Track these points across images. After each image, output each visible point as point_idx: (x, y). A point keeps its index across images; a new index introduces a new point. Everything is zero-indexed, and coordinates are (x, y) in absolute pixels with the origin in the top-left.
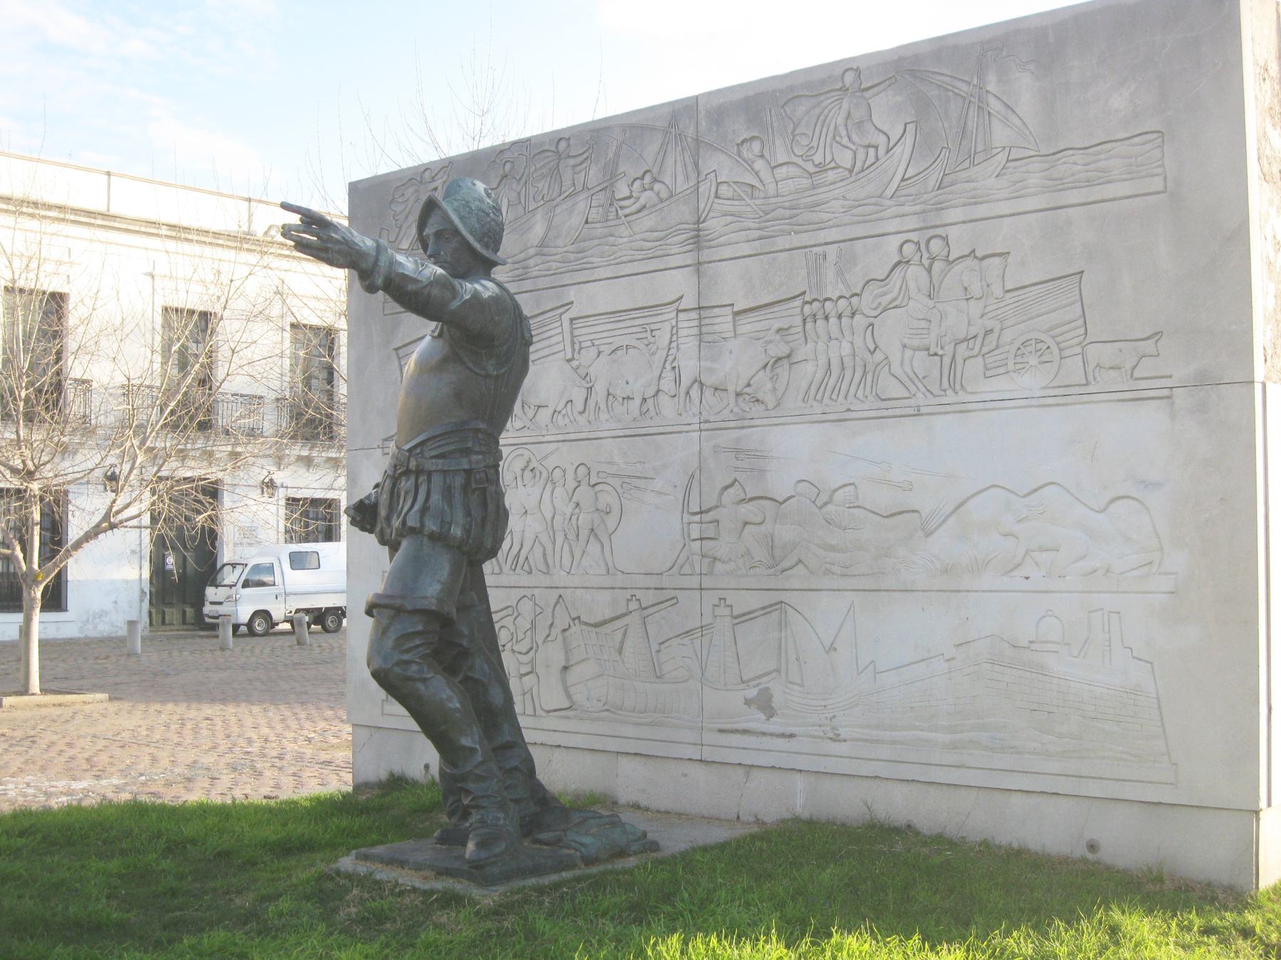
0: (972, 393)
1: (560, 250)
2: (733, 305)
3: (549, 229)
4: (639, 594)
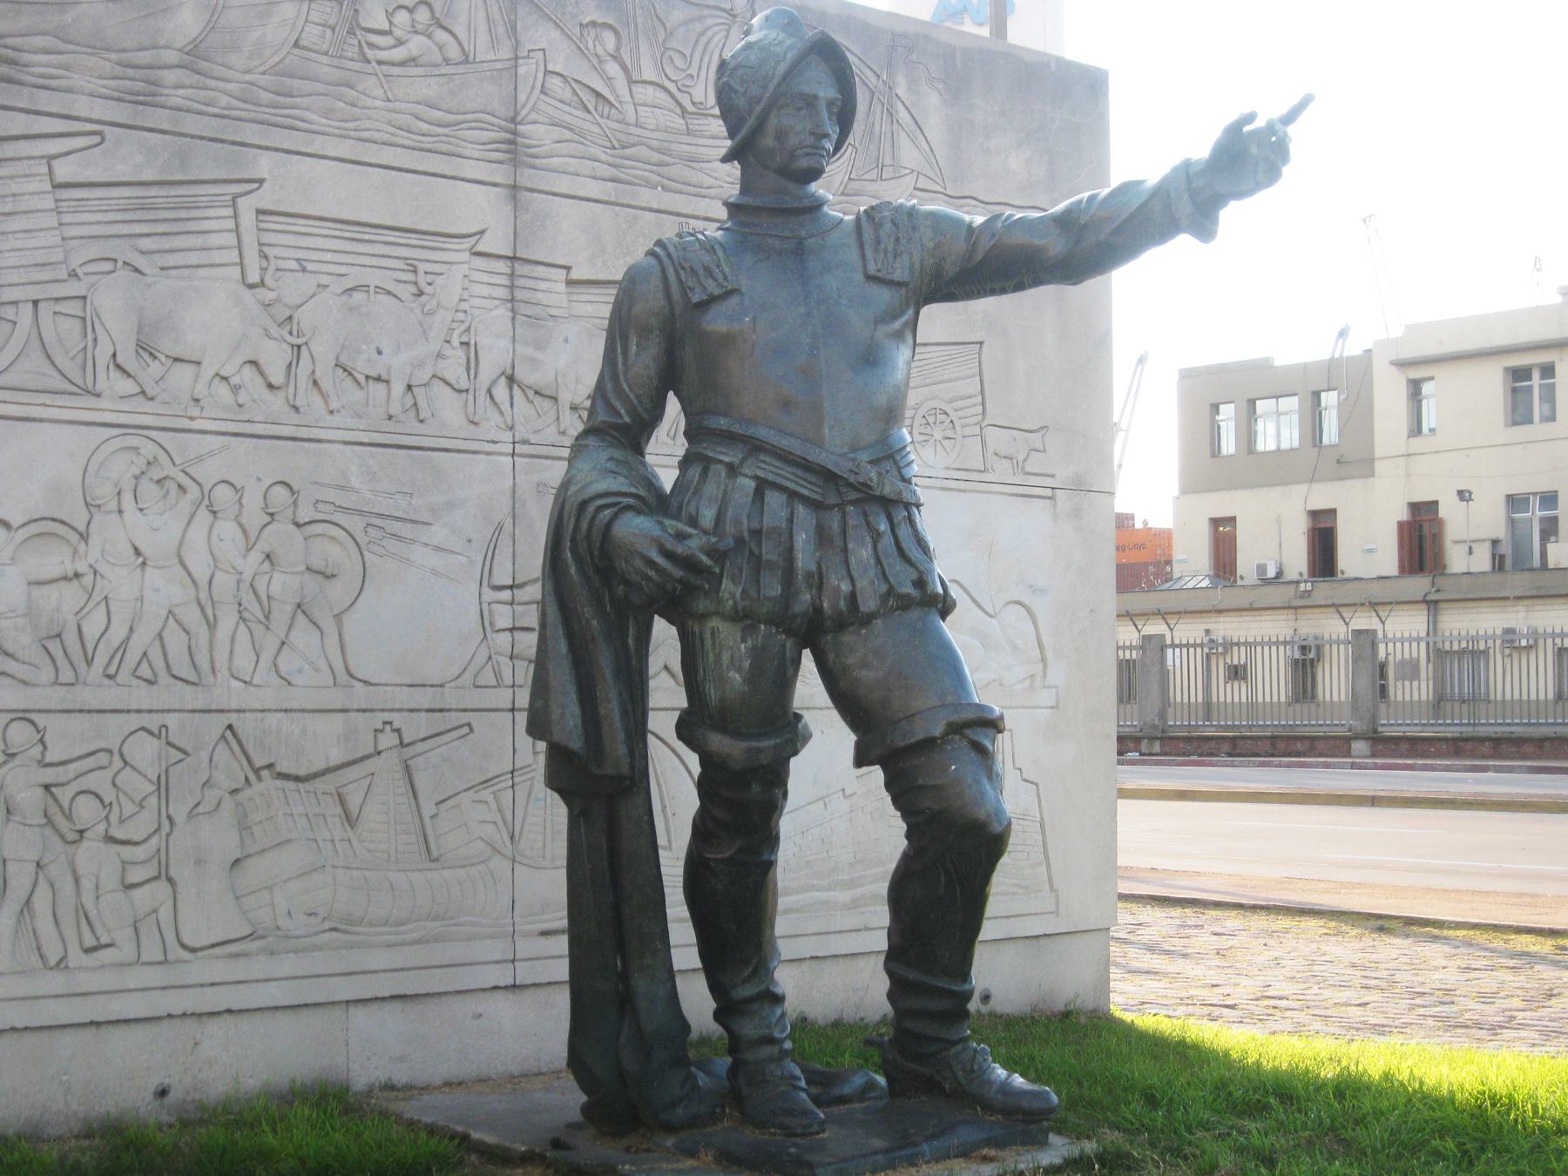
1: (238, 76)
2: (568, 268)
3: (211, 28)
4: (397, 719)
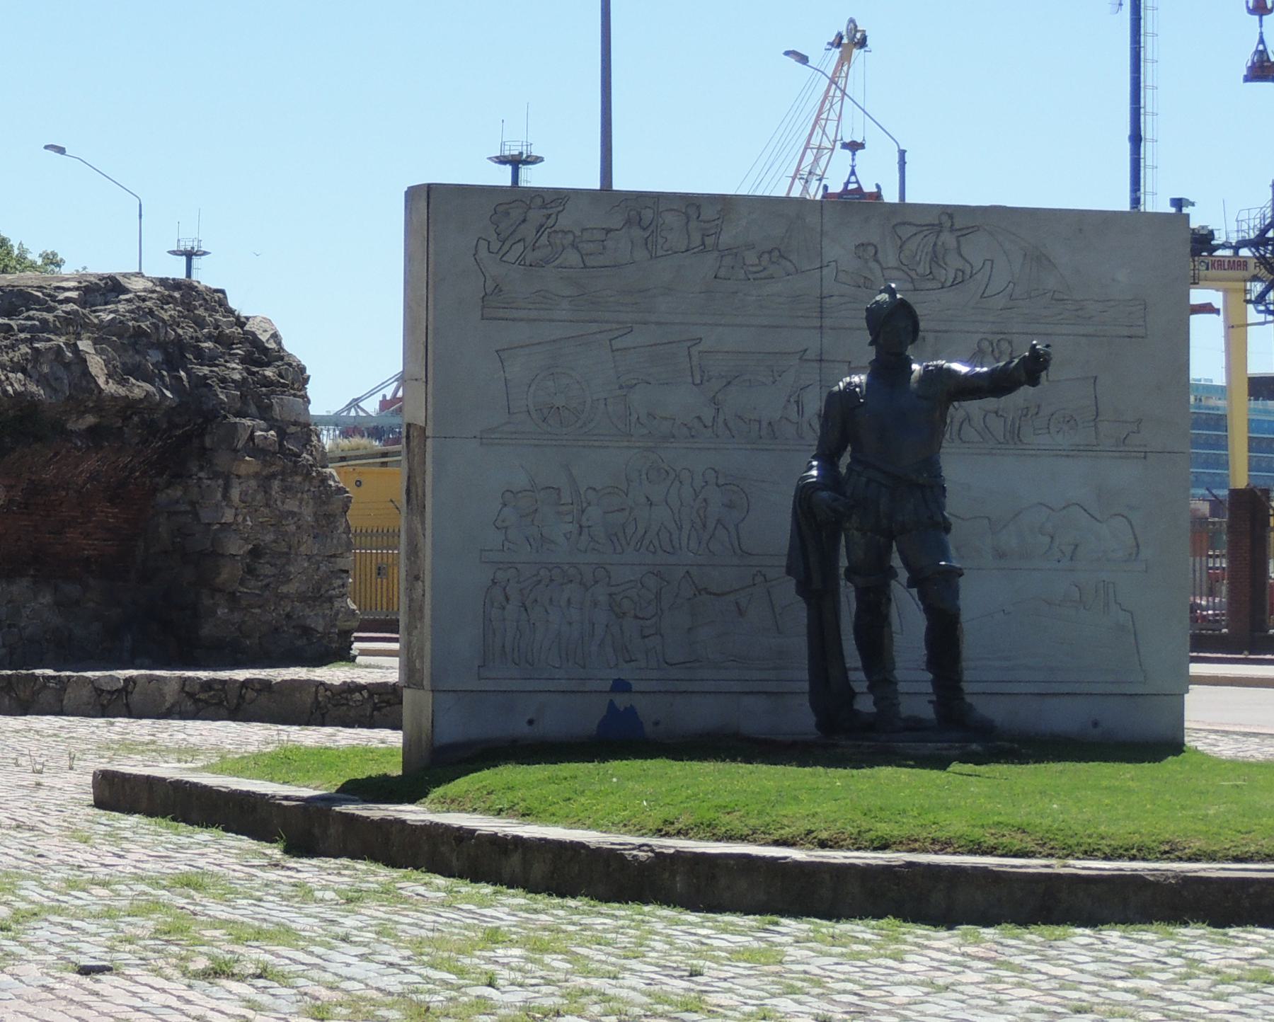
0: (1026, 444)
